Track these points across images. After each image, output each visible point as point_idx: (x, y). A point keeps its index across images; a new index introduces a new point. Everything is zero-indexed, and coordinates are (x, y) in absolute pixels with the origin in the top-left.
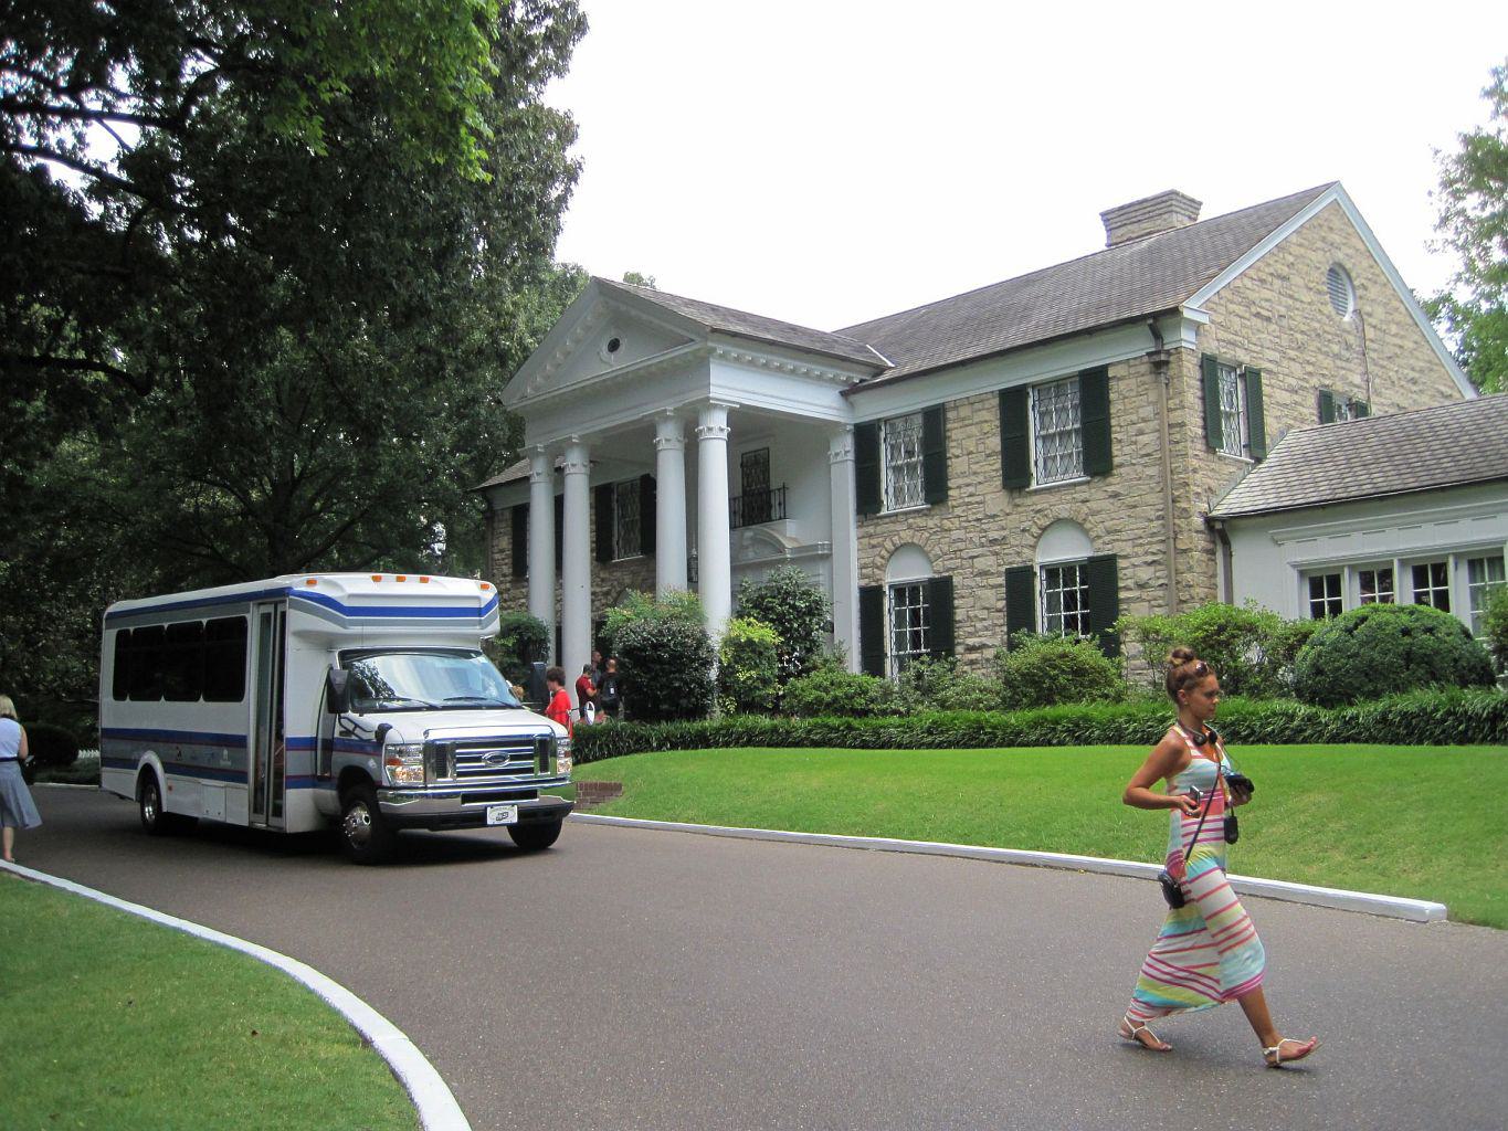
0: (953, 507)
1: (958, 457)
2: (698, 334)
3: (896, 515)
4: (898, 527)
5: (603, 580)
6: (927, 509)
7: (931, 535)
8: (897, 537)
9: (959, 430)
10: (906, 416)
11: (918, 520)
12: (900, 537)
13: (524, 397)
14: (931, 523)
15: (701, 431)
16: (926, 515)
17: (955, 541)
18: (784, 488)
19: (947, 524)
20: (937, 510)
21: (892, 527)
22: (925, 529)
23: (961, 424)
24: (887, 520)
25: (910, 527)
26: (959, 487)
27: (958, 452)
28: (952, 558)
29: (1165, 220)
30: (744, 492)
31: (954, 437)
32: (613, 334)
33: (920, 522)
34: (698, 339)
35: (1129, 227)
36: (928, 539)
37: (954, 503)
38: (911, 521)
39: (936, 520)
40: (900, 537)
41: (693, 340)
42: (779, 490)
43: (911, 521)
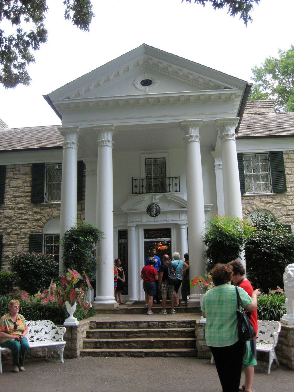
0: (288, 195)
1: (289, 174)
2: (236, 87)
3: (254, 196)
4: (255, 201)
5: (35, 213)
6: (273, 195)
7: (275, 206)
8: (255, 206)
9: (290, 163)
10: (255, 155)
11: (267, 199)
12: (256, 206)
13: (69, 98)
14: (275, 202)
15: (228, 135)
16: (272, 198)
17: (289, 210)
18: (178, 178)
19: (285, 203)
20: (279, 196)
21: (251, 201)
22: (272, 203)
23: (290, 161)
24: (248, 198)
25: (262, 202)
26: (291, 187)
27: (290, 172)
28: (288, 217)
29: (270, 110)
30: (146, 177)
31: (287, 166)
32: (147, 77)
33: (269, 200)
34: (234, 88)
35: (255, 109)
36: (273, 208)
37: (288, 194)
38: (263, 199)
39: (278, 200)
40: (256, 206)
41: (226, 88)
42: (176, 178)
43: (263, 199)
